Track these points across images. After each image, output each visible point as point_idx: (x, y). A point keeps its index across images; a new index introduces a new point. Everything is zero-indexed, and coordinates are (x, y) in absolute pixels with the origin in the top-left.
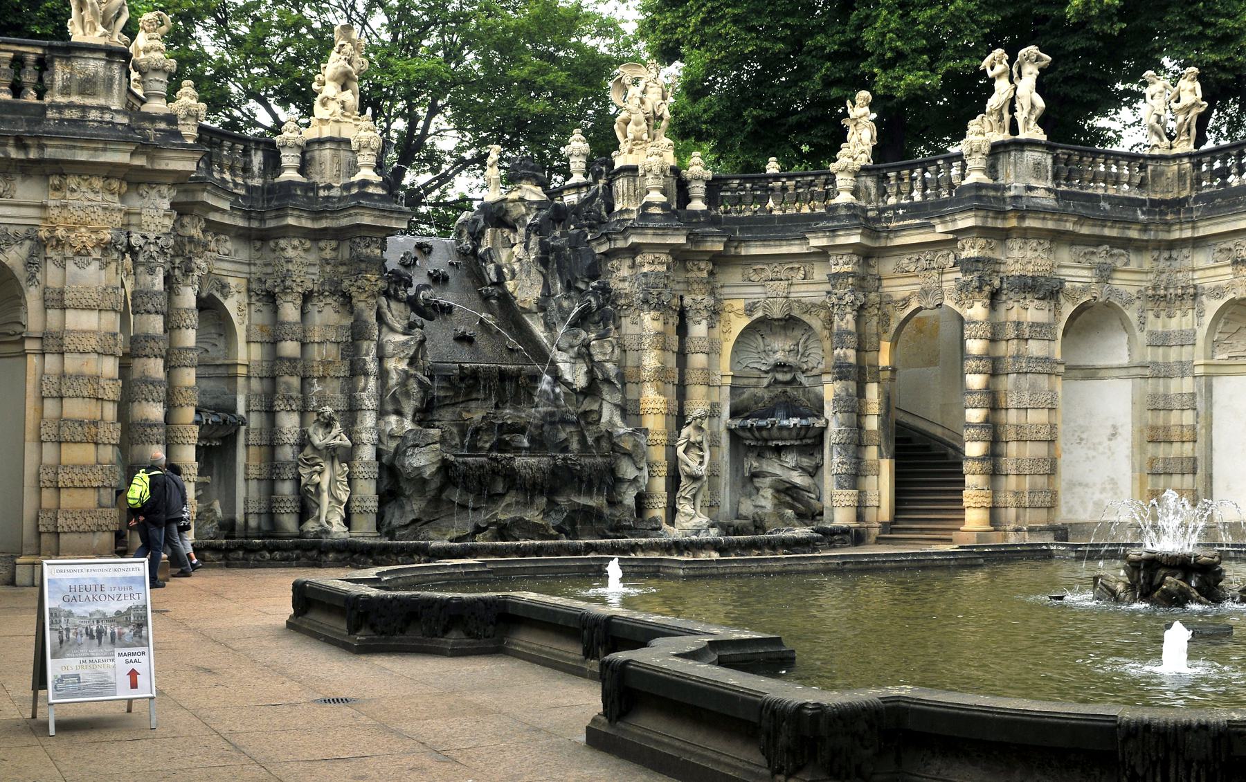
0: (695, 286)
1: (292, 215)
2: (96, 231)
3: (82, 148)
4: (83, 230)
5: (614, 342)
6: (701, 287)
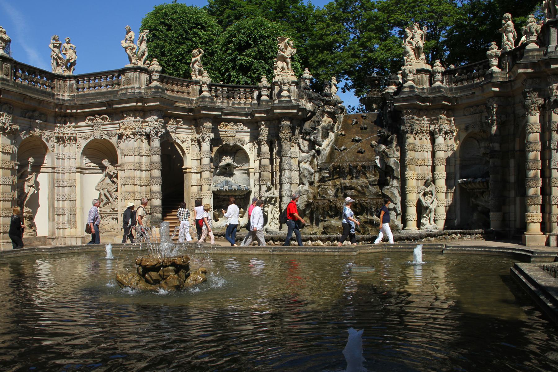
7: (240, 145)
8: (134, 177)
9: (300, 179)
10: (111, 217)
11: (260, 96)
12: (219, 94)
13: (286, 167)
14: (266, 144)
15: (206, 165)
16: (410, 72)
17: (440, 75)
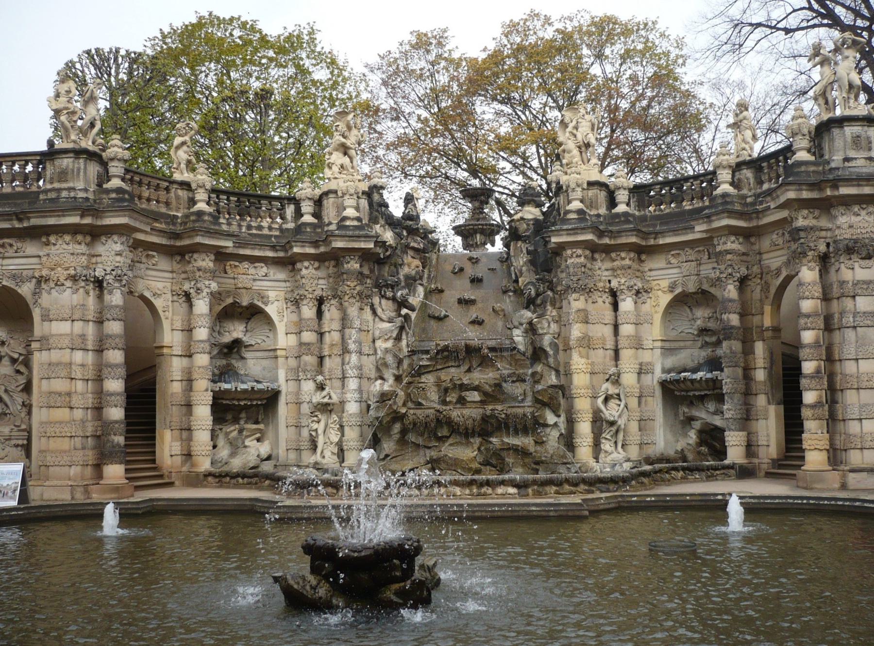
0: (619, 272)
1: (296, 246)
2: (67, 269)
3: (51, 216)
4: (59, 269)
5: (550, 319)
6: (623, 271)
7: (260, 304)
8: (70, 364)
9: (378, 369)
10: (13, 442)
11: (298, 214)
12: (223, 207)
13: (352, 346)
14: (311, 304)
15: (202, 341)
16: (578, 186)
17: (626, 192)
